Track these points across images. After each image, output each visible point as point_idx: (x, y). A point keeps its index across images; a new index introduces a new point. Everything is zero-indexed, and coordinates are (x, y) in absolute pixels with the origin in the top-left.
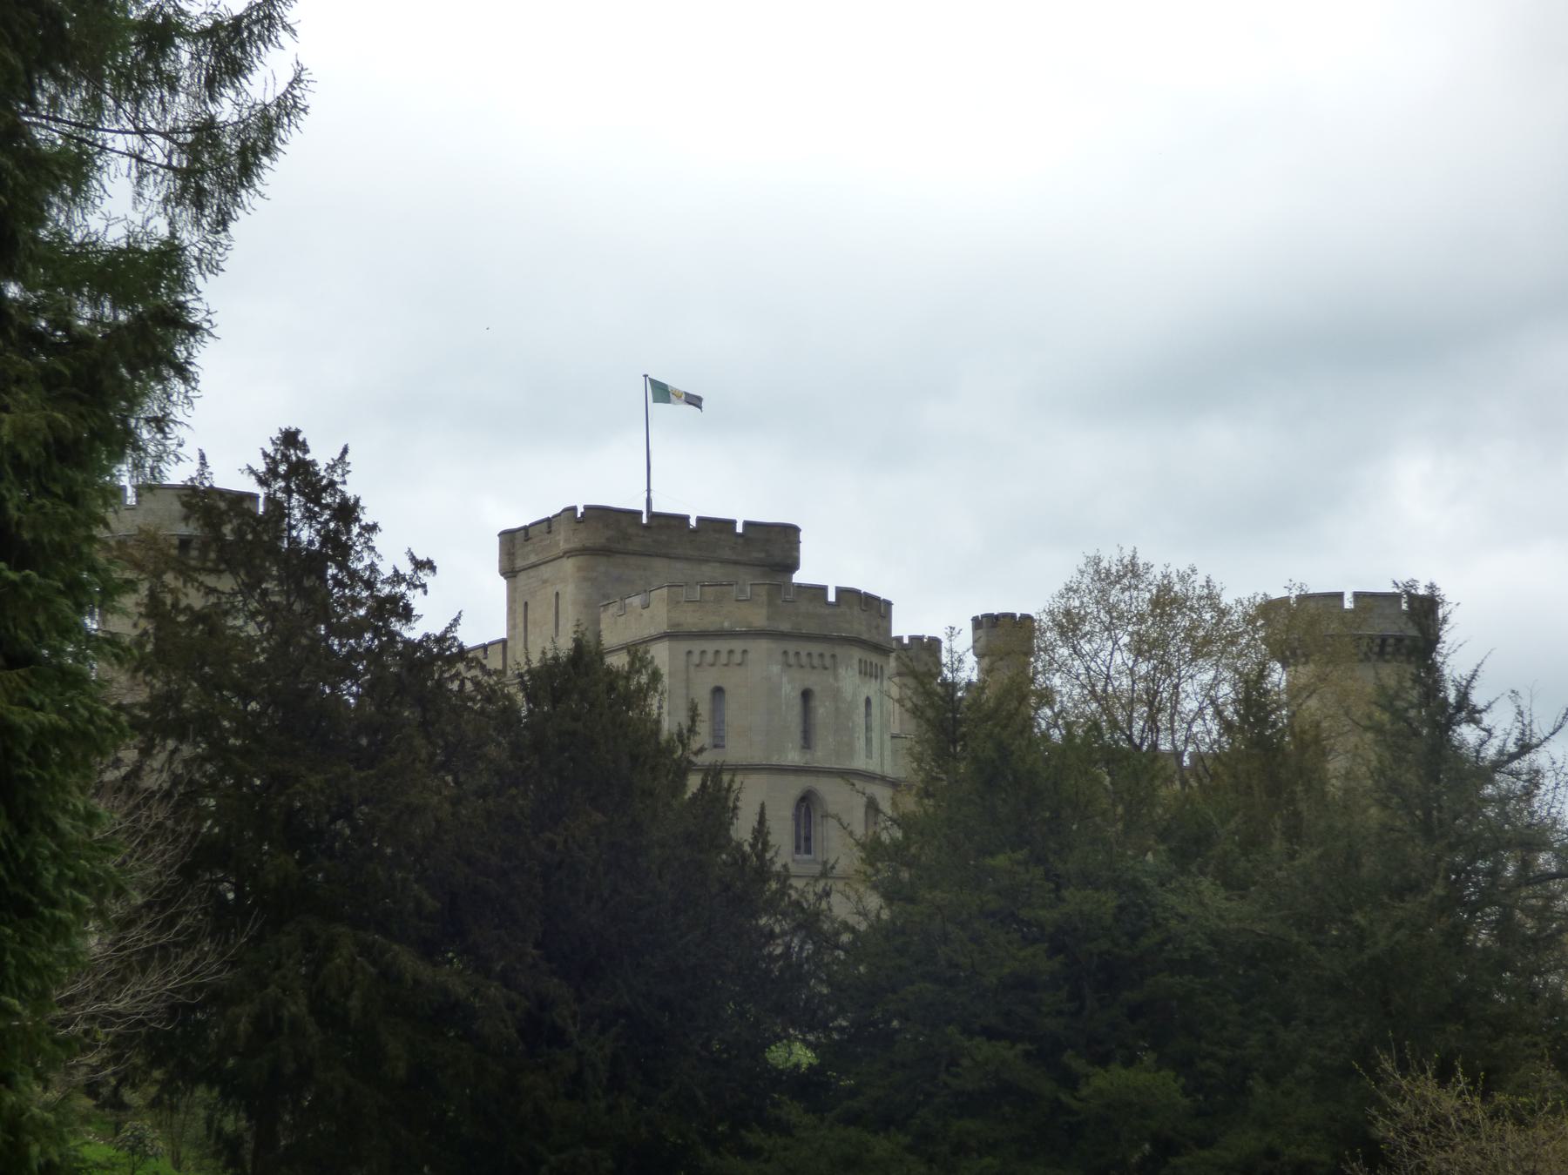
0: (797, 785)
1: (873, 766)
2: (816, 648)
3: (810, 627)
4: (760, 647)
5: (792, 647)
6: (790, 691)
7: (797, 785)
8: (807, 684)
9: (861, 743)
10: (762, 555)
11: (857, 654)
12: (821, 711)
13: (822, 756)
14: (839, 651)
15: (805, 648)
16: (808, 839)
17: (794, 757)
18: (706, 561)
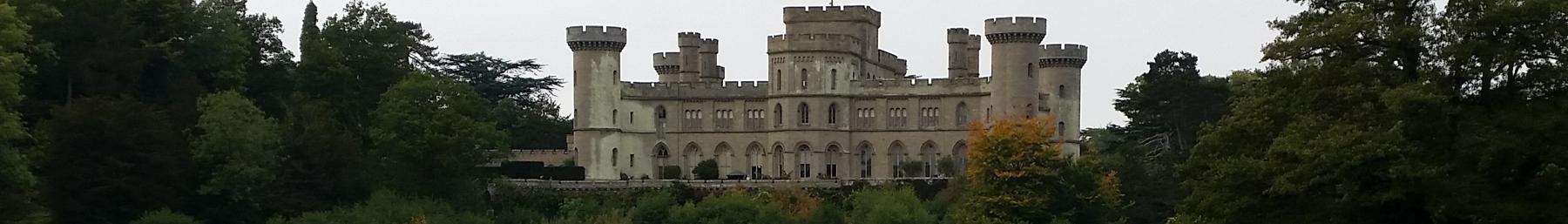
0: (799, 101)
1: (836, 92)
2: (806, 55)
3: (803, 48)
4: (787, 56)
5: (798, 55)
6: (797, 69)
7: (799, 101)
8: (804, 67)
9: (829, 84)
10: (850, 18)
11: (824, 55)
12: (809, 75)
13: (809, 91)
14: (817, 55)
15: (802, 55)
16: (807, 118)
17: (799, 92)
18: (830, 21)
